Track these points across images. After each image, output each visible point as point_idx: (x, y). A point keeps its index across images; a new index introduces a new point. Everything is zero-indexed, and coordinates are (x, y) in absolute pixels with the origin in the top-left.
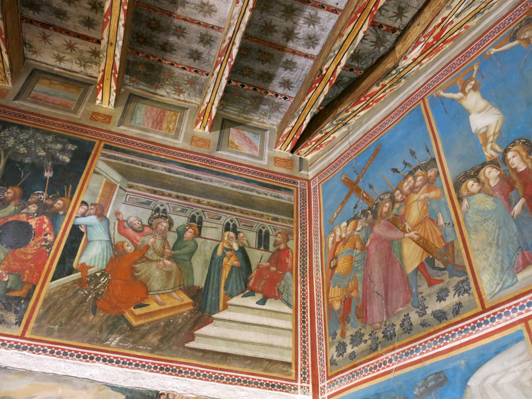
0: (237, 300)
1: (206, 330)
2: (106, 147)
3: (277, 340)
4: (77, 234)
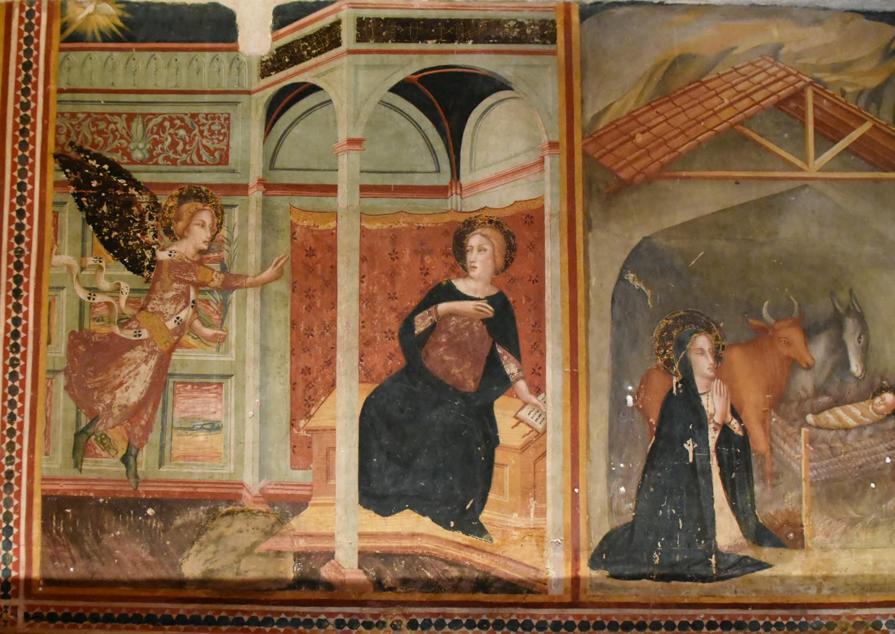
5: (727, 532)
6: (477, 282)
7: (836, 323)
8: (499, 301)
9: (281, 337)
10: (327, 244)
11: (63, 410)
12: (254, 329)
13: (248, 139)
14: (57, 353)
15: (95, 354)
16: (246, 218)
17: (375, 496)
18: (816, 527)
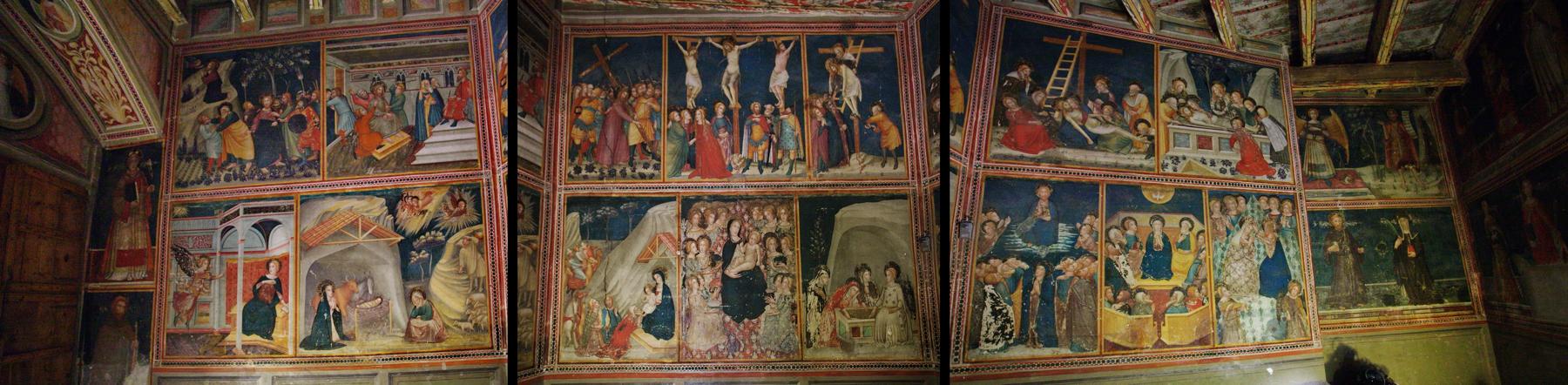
0: (438, 128)
1: (421, 152)
2: (329, 43)
3: (467, 147)
4: (330, 113)
5: (335, 337)
6: (272, 276)
7: (365, 280)
8: (278, 280)
9: (224, 291)
10: (236, 267)
11: (172, 312)
12: (217, 290)
13: (217, 241)
14: (171, 297)
15: (179, 297)
16: (216, 261)
17: (246, 331)
18: (359, 335)
